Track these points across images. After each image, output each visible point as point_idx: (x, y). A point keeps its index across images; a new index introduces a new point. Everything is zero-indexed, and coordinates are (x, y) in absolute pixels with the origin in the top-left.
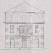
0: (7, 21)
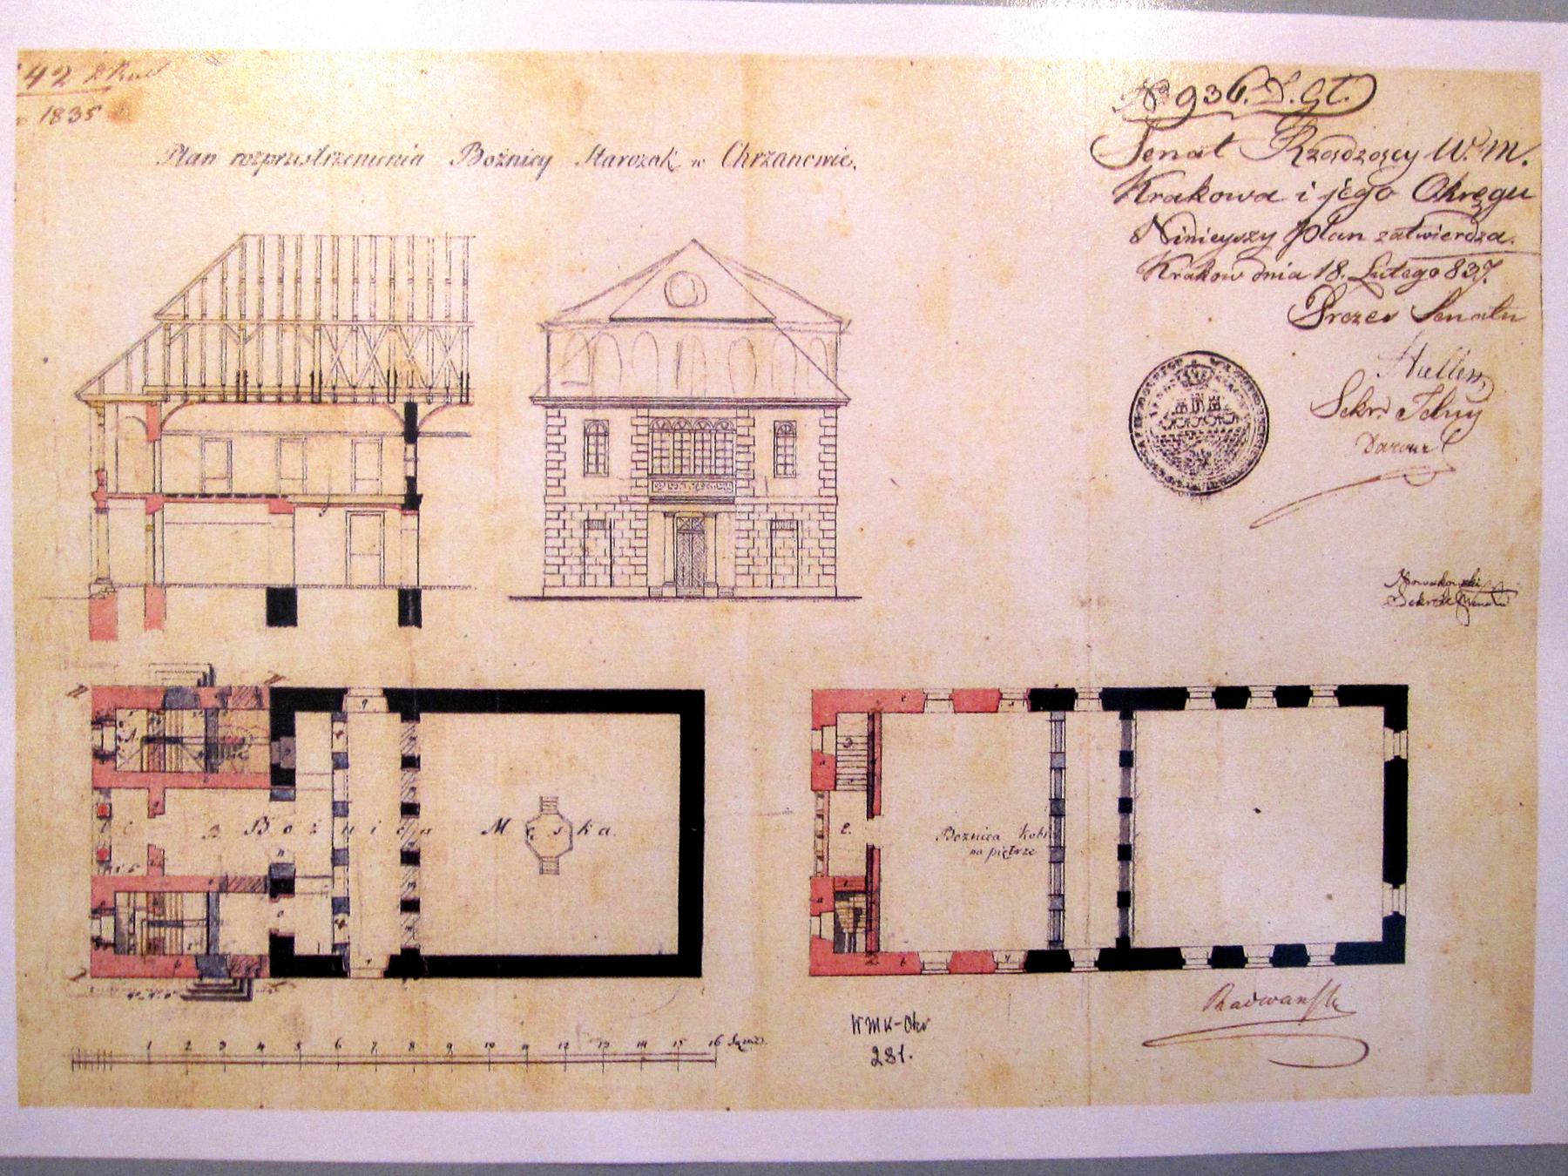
0: (557, 391)
